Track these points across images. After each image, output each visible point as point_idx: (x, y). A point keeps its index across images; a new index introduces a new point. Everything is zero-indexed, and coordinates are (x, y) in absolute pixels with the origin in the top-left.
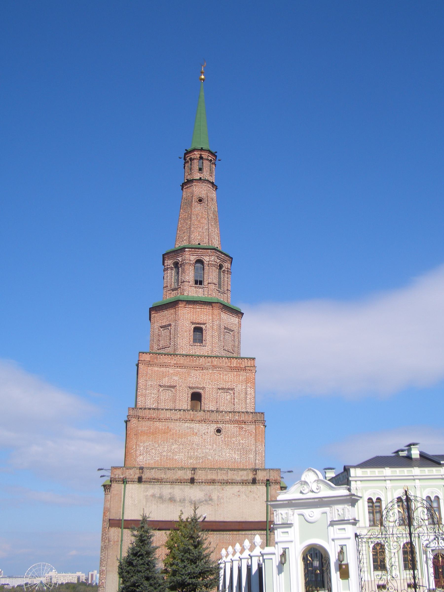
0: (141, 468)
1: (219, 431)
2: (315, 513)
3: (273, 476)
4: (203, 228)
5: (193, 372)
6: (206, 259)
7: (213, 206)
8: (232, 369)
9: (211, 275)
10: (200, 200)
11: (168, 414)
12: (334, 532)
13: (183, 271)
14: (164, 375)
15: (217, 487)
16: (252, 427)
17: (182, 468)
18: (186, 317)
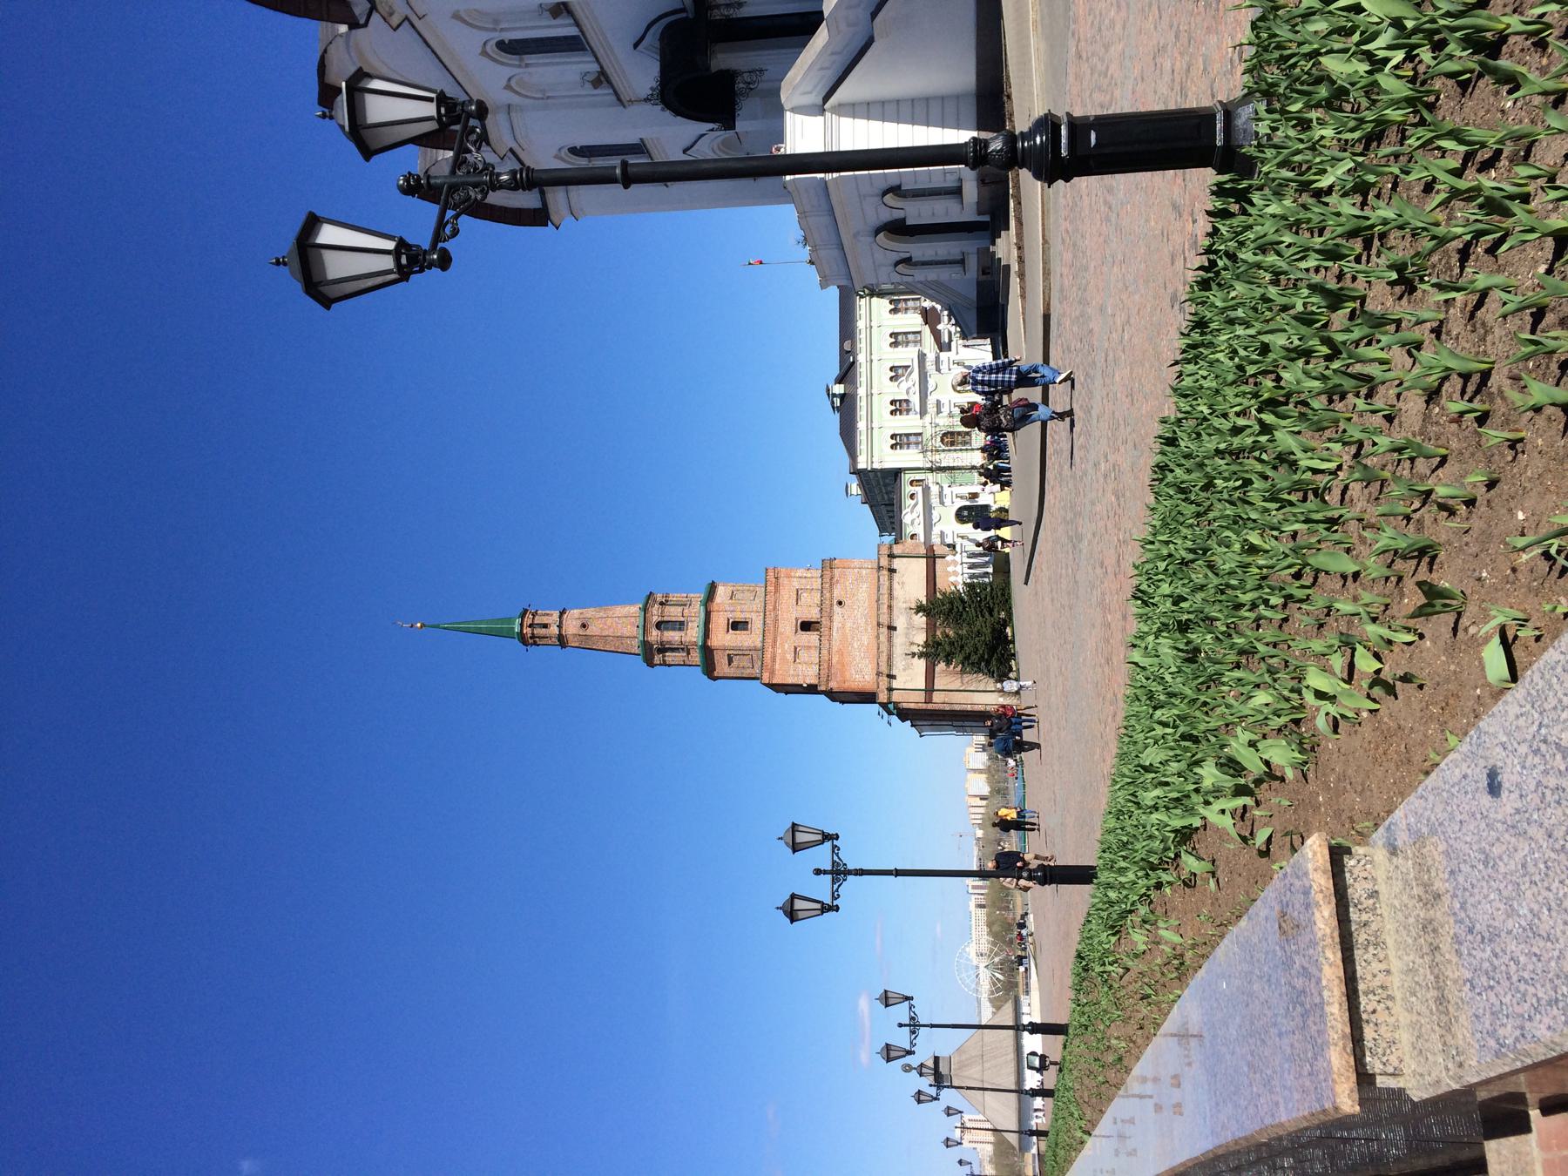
0: (878, 674)
1: (840, 603)
2: (935, 514)
3: (885, 551)
4: (620, 621)
5: (781, 629)
6: (655, 619)
7: (590, 613)
8: (777, 590)
9: (673, 613)
10: (584, 626)
11: (824, 652)
12: (947, 501)
13: (669, 643)
14: (784, 659)
15: (894, 603)
16: (837, 572)
17: (878, 637)
18: (722, 638)
